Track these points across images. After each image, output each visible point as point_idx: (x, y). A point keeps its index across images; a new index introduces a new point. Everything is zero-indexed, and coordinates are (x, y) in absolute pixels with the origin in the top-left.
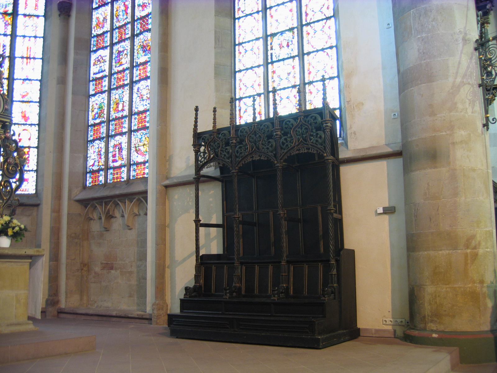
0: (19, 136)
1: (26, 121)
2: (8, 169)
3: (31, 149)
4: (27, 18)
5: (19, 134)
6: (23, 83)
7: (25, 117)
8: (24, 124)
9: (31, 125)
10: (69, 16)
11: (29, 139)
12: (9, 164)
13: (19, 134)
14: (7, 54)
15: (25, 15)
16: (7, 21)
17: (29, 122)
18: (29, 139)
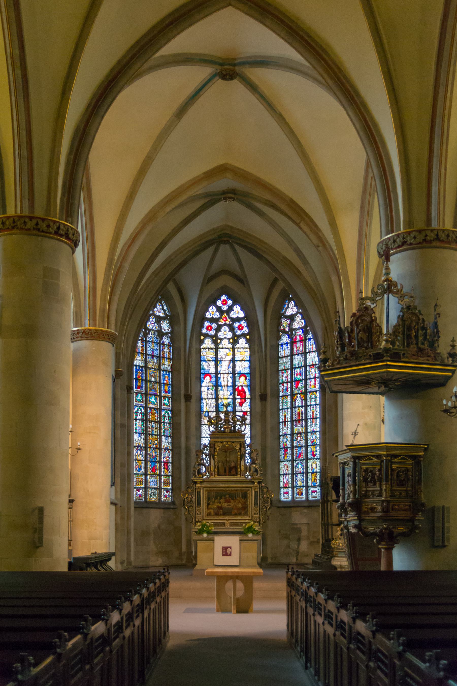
0: (311, 466)
1: (314, 457)
2: (264, 501)
3: (317, 473)
4: (311, 393)
5: (312, 465)
6: (312, 434)
7: (314, 455)
8: (314, 459)
9: (316, 459)
10: (326, 391)
11: (316, 467)
12: (264, 498)
13: (312, 465)
14: (304, 418)
15: (310, 392)
16: (302, 398)
17: (316, 458)
18: (316, 467)
